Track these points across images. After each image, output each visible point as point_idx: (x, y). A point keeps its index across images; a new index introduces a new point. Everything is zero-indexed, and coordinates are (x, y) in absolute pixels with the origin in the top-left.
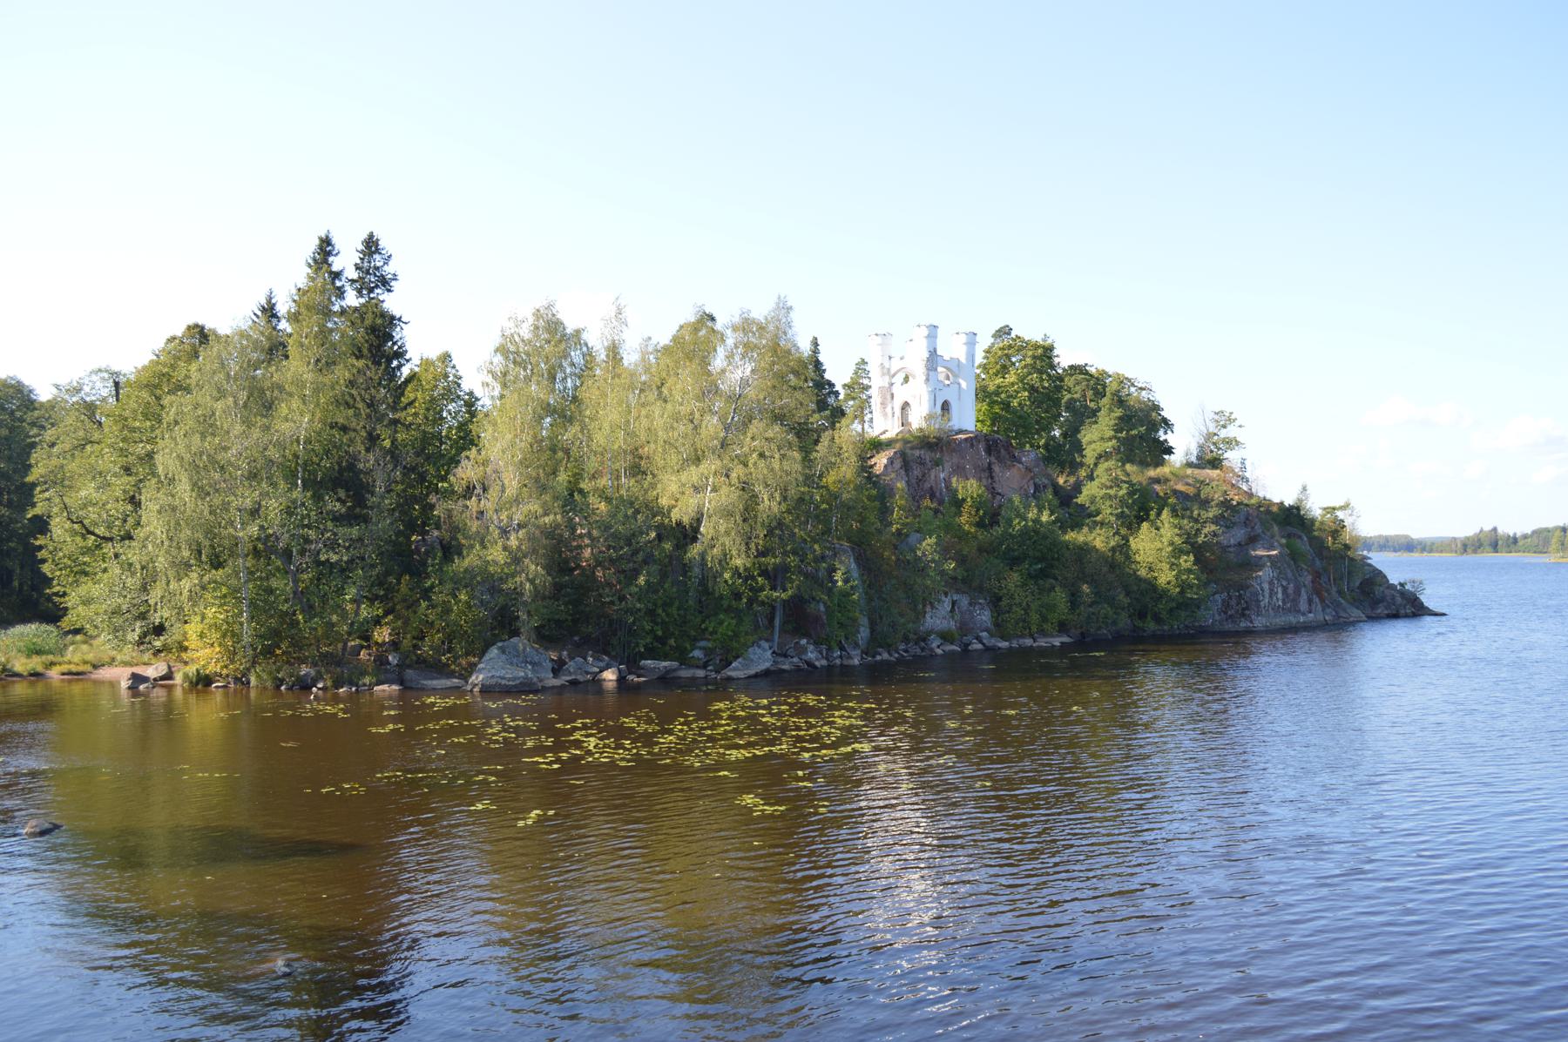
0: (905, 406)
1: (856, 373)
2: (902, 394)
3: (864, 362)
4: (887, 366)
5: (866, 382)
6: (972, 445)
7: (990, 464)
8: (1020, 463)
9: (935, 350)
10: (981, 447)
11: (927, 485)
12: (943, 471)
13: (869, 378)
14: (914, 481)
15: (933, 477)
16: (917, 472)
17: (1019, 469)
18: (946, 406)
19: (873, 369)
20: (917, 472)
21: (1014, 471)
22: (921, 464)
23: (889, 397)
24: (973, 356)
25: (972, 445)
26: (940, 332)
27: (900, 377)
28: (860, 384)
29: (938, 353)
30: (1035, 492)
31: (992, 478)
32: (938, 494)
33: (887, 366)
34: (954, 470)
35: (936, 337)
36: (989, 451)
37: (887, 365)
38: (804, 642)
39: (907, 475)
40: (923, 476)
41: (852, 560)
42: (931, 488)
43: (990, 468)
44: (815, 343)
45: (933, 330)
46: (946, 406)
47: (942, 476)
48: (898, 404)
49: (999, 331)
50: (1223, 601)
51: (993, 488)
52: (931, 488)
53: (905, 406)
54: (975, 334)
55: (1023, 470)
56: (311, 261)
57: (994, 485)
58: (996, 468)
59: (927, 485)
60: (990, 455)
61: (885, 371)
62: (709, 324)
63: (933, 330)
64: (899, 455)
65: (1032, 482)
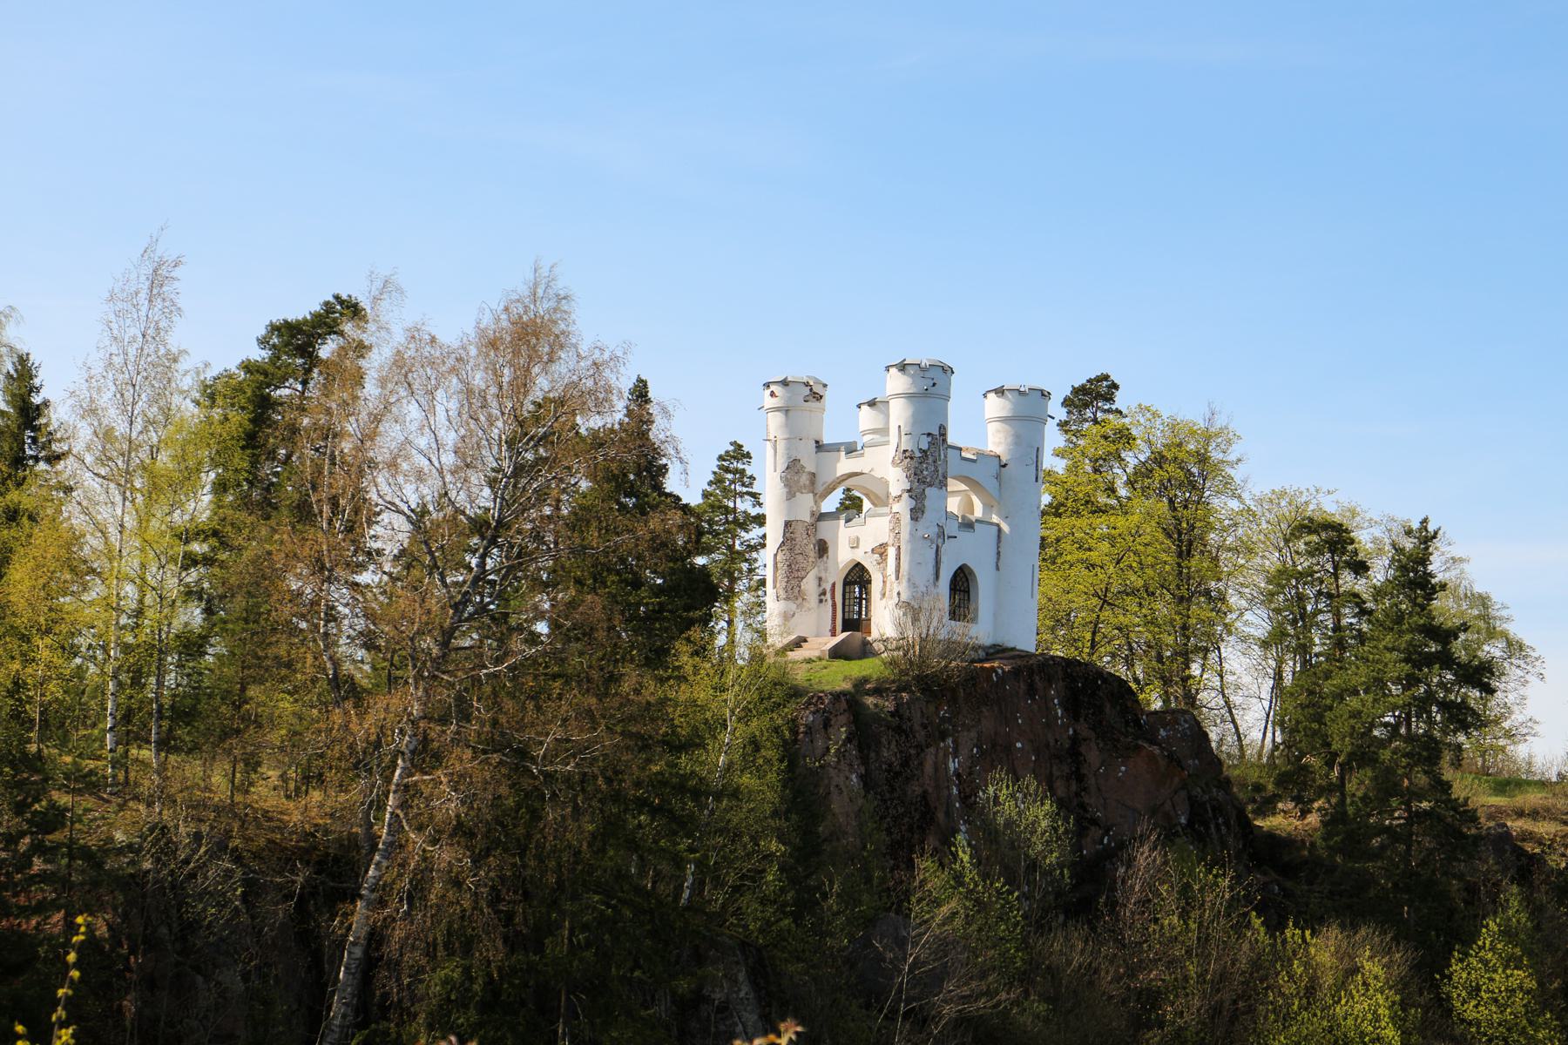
1: (718, 481)
3: (739, 453)
4: (810, 468)
5: (744, 505)
6: (1031, 690)
7: (1075, 741)
8: (1153, 742)
11: (915, 789)
12: (955, 756)
13: (754, 495)
15: (929, 768)
16: (889, 753)
17: (1152, 757)
18: (962, 583)
19: (767, 475)
20: (889, 753)
22: (899, 730)
23: (811, 550)
24: (1038, 452)
27: (831, 504)
28: (727, 510)
29: (952, 439)
30: (1190, 823)
31: (1080, 778)
32: (941, 816)
33: (810, 467)
34: (982, 752)
35: (947, 398)
36: (1073, 706)
37: (809, 464)
39: (865, 760)
40: (905, 763)
41: (741, 976)
42: (924, 795)
43: (1074, 752)
44: (641, 393)
46: (962, 583)
47: (952, 765)
49: (1076, 391)
51: (1083, 806)
52: (924, 795)
53: (858, 578)
54: (1045, 395)
55: (1163, 763)
57: (1086, 800)
58: (1093, 754)
59: (915, 789)
60: (1076, 718)
61: (804, 479)
62: (348, 327)
64: (844, 705)
65: (1183, 794)
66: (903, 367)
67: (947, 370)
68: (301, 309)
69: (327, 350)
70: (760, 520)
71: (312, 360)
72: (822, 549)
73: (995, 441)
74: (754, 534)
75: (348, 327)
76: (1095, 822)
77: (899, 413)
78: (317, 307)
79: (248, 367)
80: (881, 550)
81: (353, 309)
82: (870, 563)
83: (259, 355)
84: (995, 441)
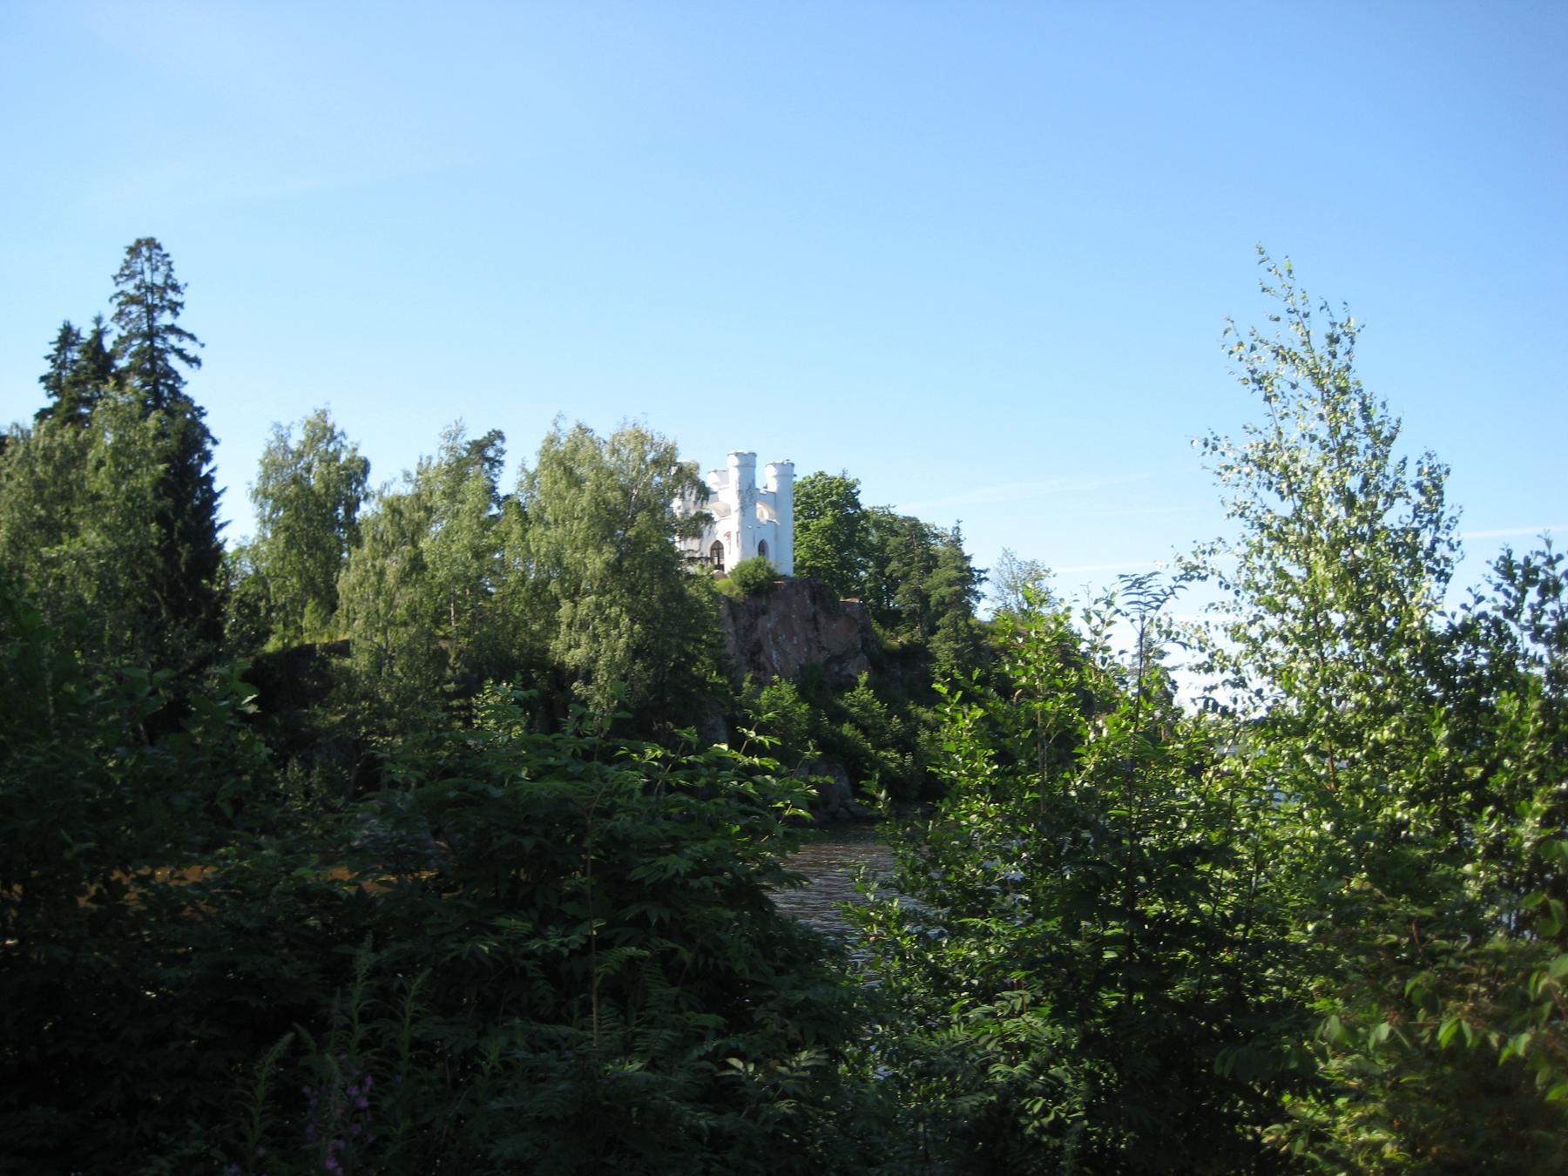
6: (797, 593)
7: (815, 614)
9: (754, 481)
10: (806, 593)
11: (755, 636)
14: (741, 632)
15: (760, 627)
26: (759, 462)
31: (817, 630)
32: (765, 648)
36: (814, 599)
40: (751, 625)
43: (814, 619)
45: (747, 463)
46: (762, 548)
47: (769, 625)
51: (819, 642)
58: (822, 620)
59: (755, 636)
62: (498, 442)
63: (747, 463)
66: (737, 454)
67: (754, 455)
68: (479, 438)
73: (773, 487)
75: (498, 442)
76: (824, 648)
77: (734, 475)
78: (486, 435)
80: (728, 535)
81: (499, 435)
82: (723, 541)
84: (773, 487)
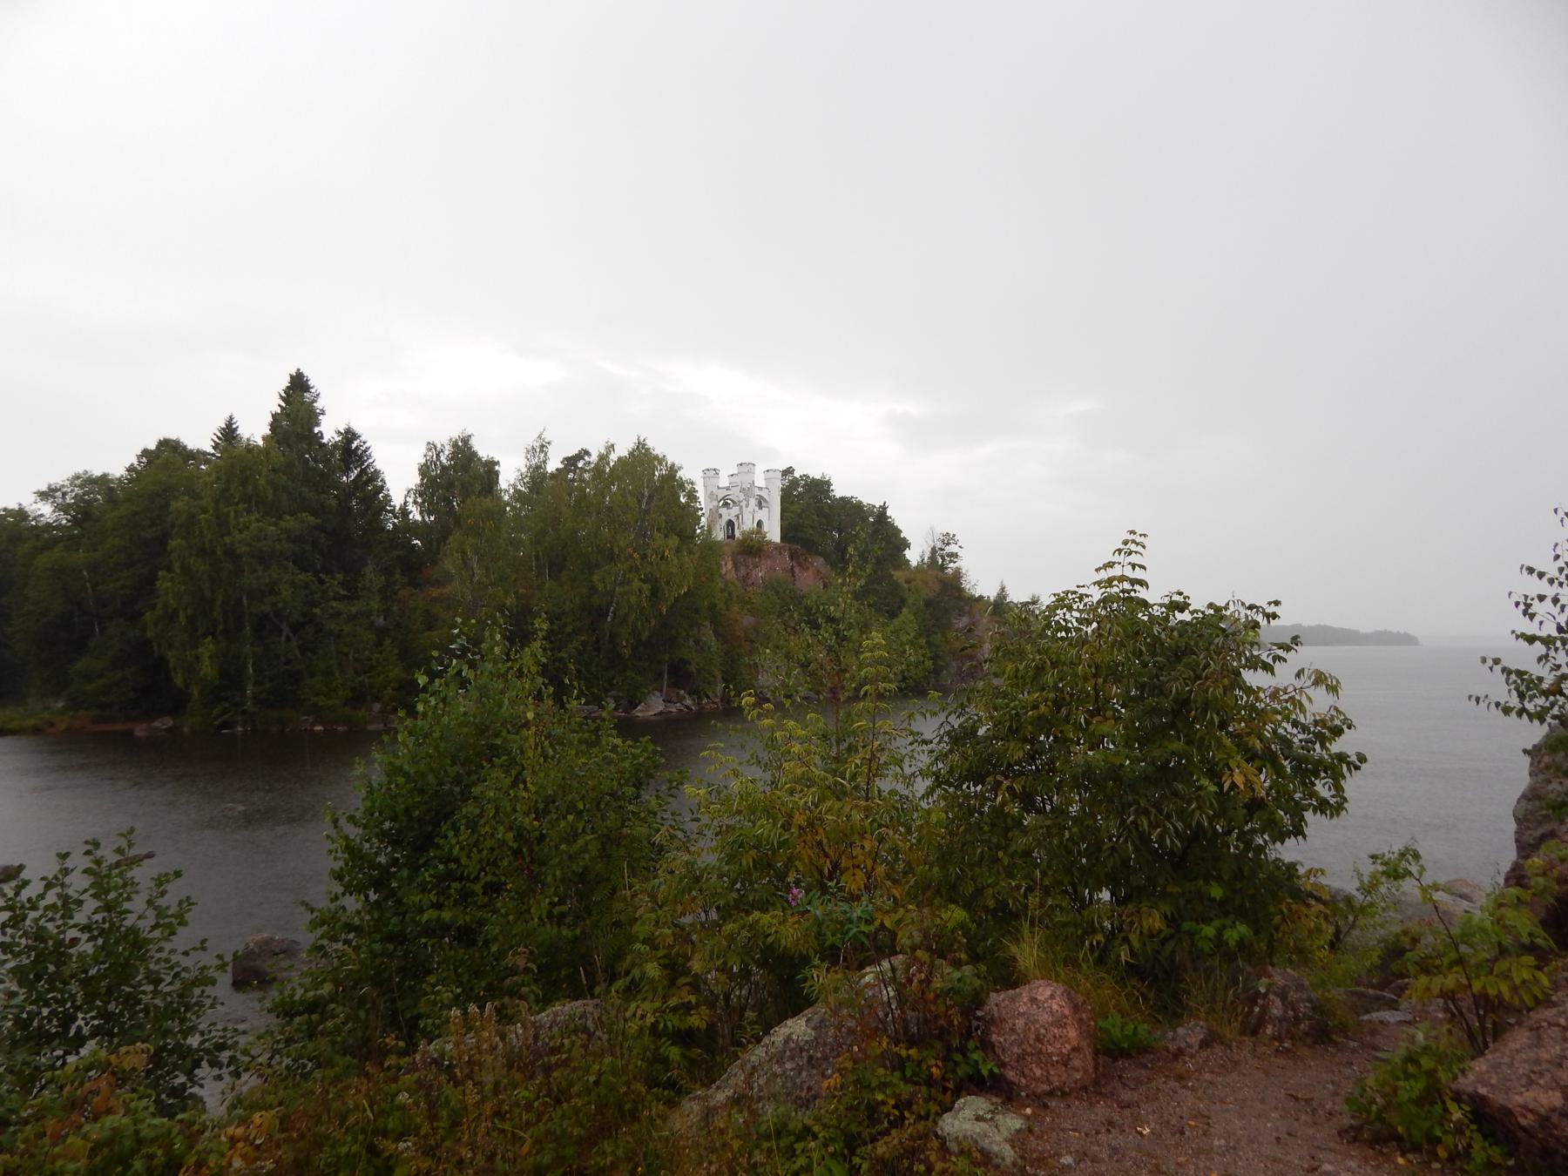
0: (730, 524)
2: (727, 514)
6: (780, 554)
16: (743, 571)
18: (760, 524)
20: (743, 571)
21: (810, 572)
25: (780, 554)
31: (793, 576)
36: (791, 558)
38: (682, 692)
43: (792, 571)
46: (760, 524)
47: (760, 575)
48: (723, 522)
50: (958, 667)
53: (730, 524)
56: (283, 395)
58: (797, 570)
62: (586, 458)
68: (572, 452)
69: (580, 464)
70: (701, 509)
71: (576, 467)
72: (721, 516)
74: (700, 513)
75: (586, 458)
79: (557, 470)
80: (737, 516)
82: (734, 520)
83: (561, 466)
